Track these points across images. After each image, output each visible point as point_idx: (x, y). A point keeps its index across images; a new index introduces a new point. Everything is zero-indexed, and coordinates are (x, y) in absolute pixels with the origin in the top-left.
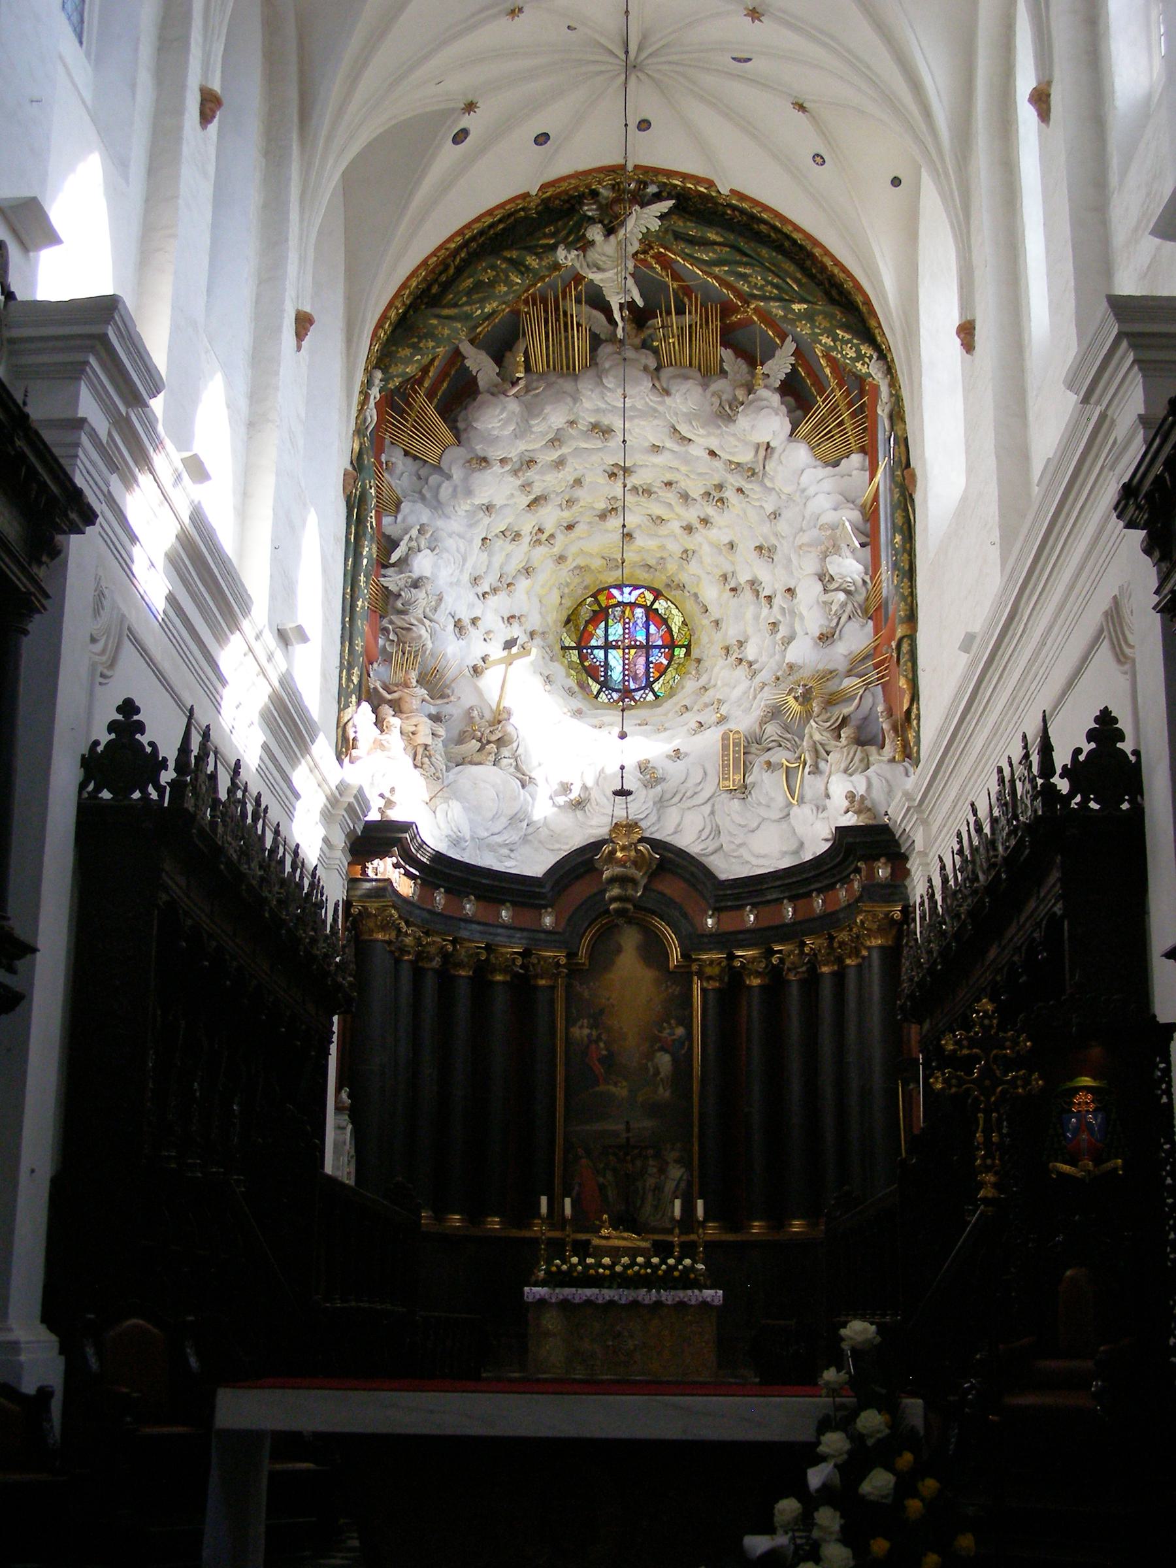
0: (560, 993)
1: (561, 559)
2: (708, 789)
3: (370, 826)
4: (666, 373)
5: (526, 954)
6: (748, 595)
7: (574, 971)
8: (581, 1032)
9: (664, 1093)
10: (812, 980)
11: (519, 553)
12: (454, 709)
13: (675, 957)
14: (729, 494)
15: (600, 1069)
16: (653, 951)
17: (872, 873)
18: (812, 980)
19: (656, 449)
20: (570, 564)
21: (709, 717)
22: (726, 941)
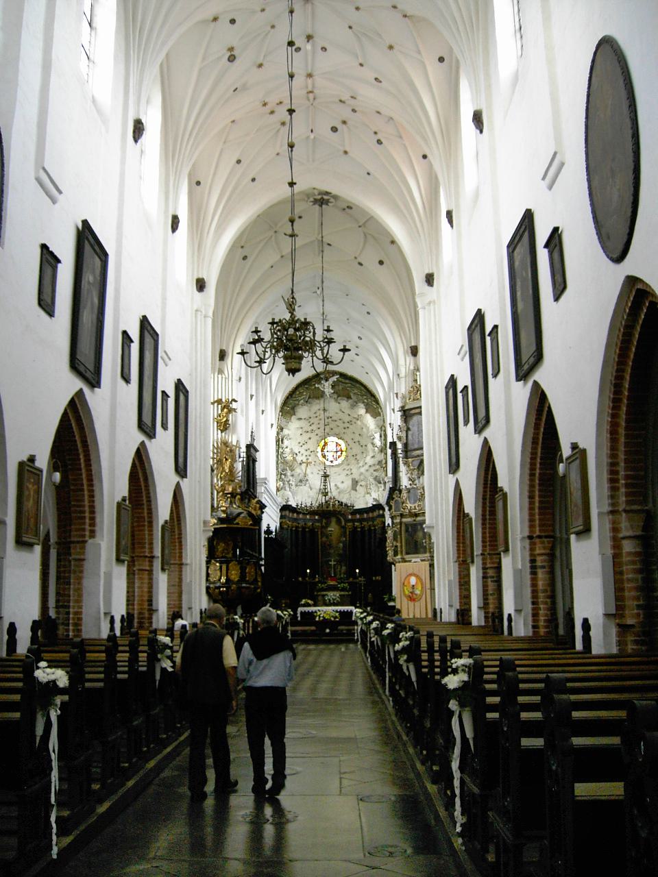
0: (319, 533)
1: (317, 435)
2: (349, 490)
3: (284, 505)
4: (339, 398)
5: (313, 524)
6: (358, 443)
7: (322, 527)
8: (324, 539)
9: (341, 552)
10: (370, 530)
11: (309, 435)
12: (296, 474)
13: (343, 523)
14: (353, 423)
15: (328, 547)
16: (339, 522)
17: (379, 512)
18: (370, 530)
19: (337, 413)
20: (319, 435)
21: (349, 473)
22: (353, 521)
